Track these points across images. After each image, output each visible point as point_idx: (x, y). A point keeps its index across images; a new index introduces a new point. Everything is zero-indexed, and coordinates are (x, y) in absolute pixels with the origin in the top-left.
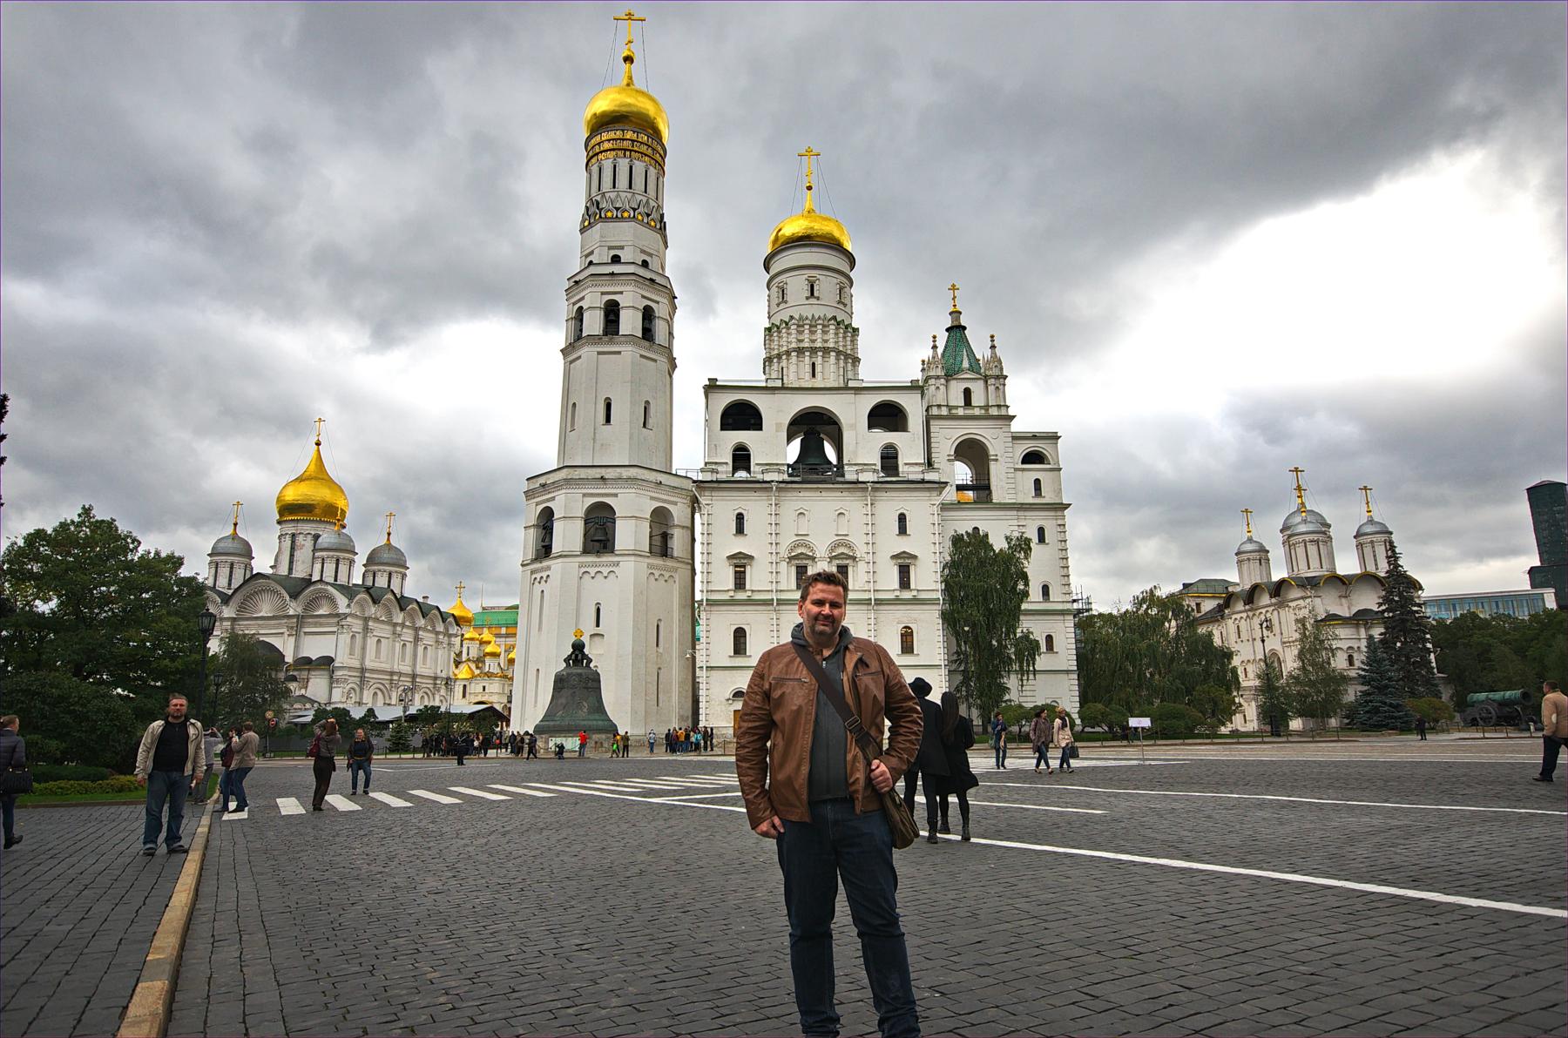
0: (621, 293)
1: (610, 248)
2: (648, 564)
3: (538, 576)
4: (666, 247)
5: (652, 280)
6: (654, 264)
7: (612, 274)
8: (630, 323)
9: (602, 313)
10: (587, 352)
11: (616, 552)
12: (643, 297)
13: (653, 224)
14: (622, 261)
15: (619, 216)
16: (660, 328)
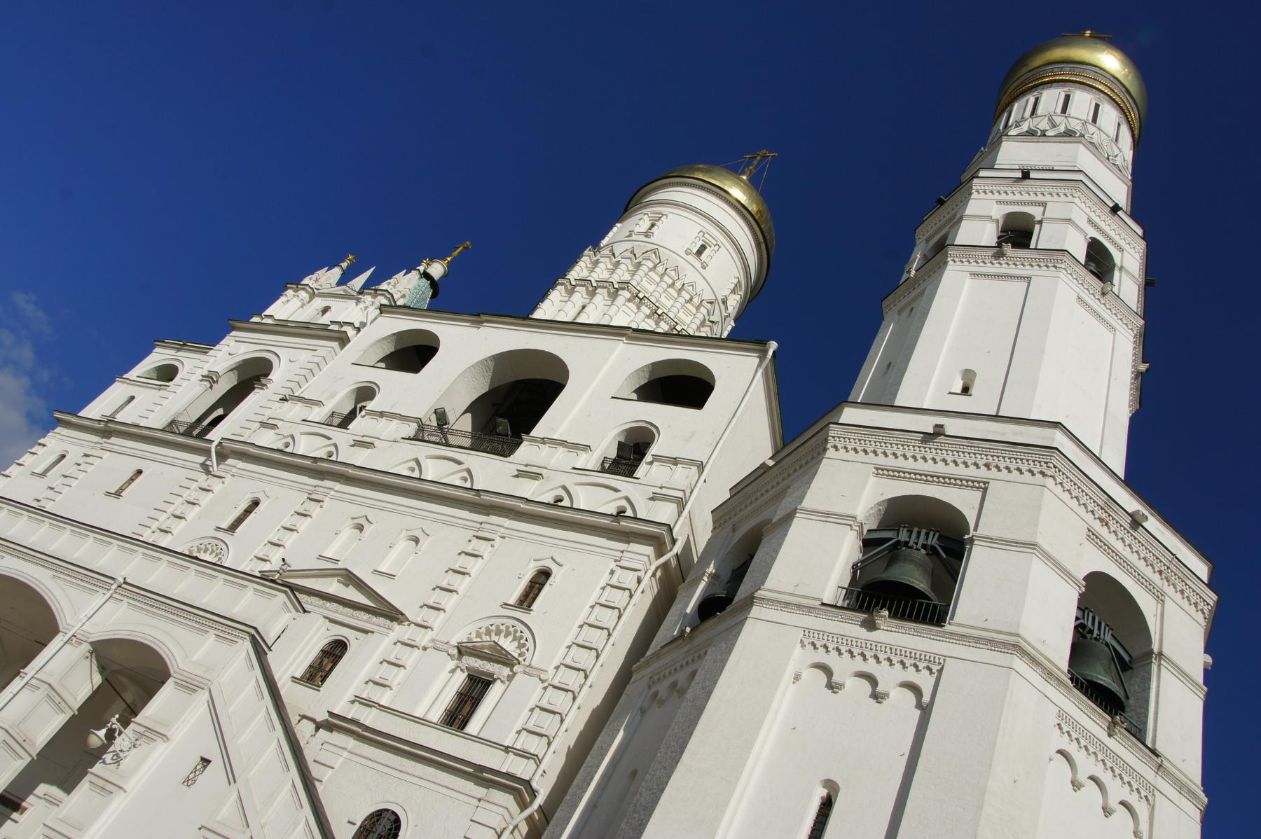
2: (1062, 714)
11: (948, 627)
12: (1090, 221)
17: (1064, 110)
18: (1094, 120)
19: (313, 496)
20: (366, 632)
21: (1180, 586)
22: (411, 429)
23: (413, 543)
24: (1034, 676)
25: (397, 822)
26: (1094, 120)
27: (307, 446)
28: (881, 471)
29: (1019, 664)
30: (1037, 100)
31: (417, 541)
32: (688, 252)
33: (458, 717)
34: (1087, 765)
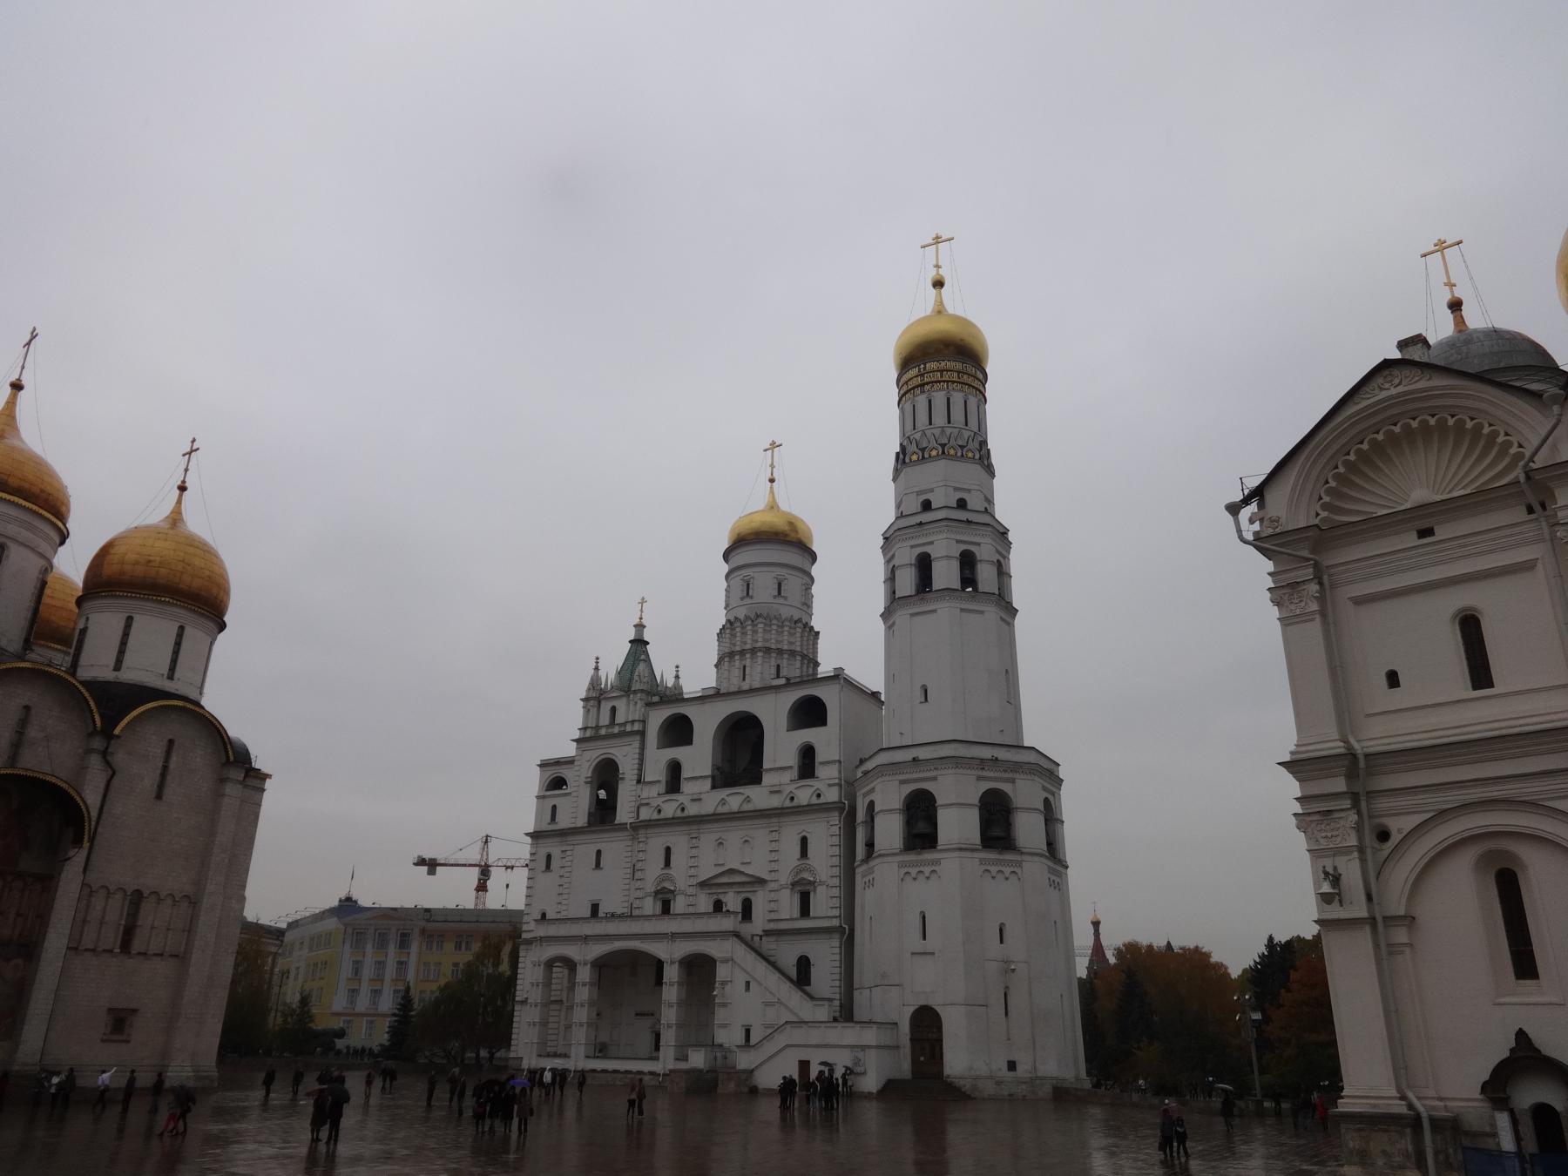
0: (931, 543)
1: (919, 493)
3: (866, 879)
4: (992, 475)
5: (968, 522)
6: (974, 502)
7: (921, 524)
8: (945, 574)
9: (913, 568)
10: (901, 616)
11: (938, 848)
12: (958, 541)
13: (970, 455)
14: (934, 506)
15: (926, 456)
16: (986, 576)
17: (930, 423)
18: (949, 422)
19: (694, 836)
20: (755, 891)
21: (1020, 771)
22: (708, 783)
23: (747, 844)
24: (968, 854)
25: (806, 956)
26: (949, 422)
27: (670, 810)
28: (902, 782)
29: (963, 854)
30: (914, 406)
31: (746, 841)
32: (775, 597)
33: (805, 911)
34: (994, 869)
